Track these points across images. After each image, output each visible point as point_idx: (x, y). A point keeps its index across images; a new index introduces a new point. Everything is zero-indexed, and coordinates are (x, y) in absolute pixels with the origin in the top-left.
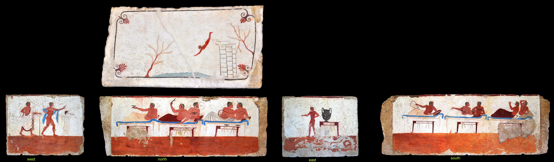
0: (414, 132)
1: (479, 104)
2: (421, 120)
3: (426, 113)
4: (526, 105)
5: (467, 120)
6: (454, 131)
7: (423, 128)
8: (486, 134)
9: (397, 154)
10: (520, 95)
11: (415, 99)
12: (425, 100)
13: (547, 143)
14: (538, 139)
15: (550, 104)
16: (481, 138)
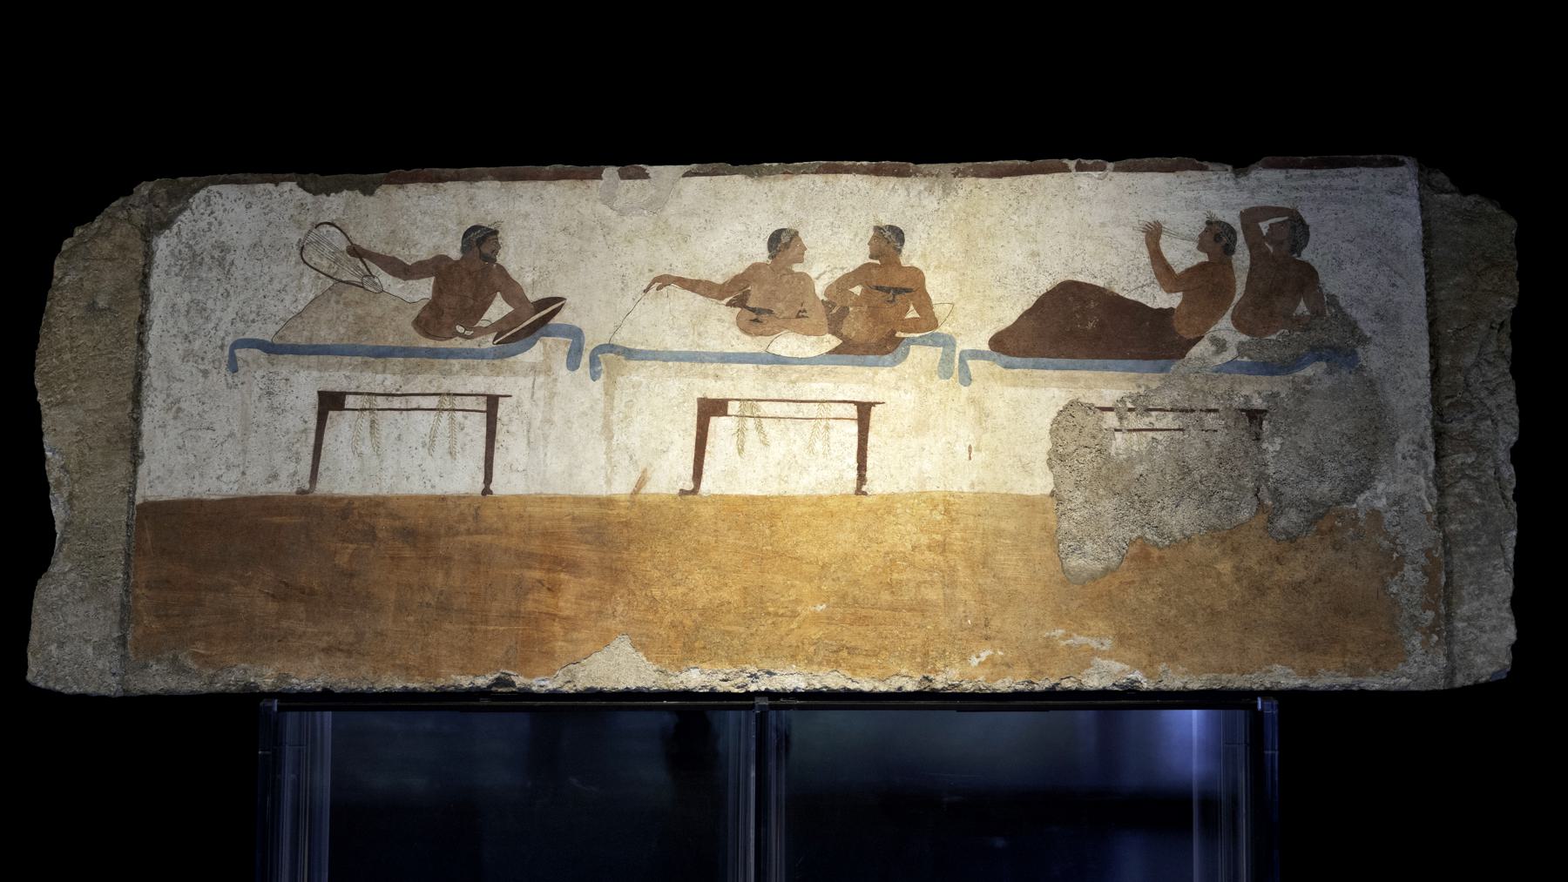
0: (323, 487)
1: (889, 239)
2: (390, 382)
3: (431, 321)
4: (1297, 247)
5: (780, 386)
6: (671, 474)
7: (409, 456)
8: (948, 506)
9: (157, 680)
10: (1240, 161)
11: (336, 204)
12: (428, 215)
13: (1503, 580)
14: (1413, 548)
15: (1520, 240)
16: (902, 535)
